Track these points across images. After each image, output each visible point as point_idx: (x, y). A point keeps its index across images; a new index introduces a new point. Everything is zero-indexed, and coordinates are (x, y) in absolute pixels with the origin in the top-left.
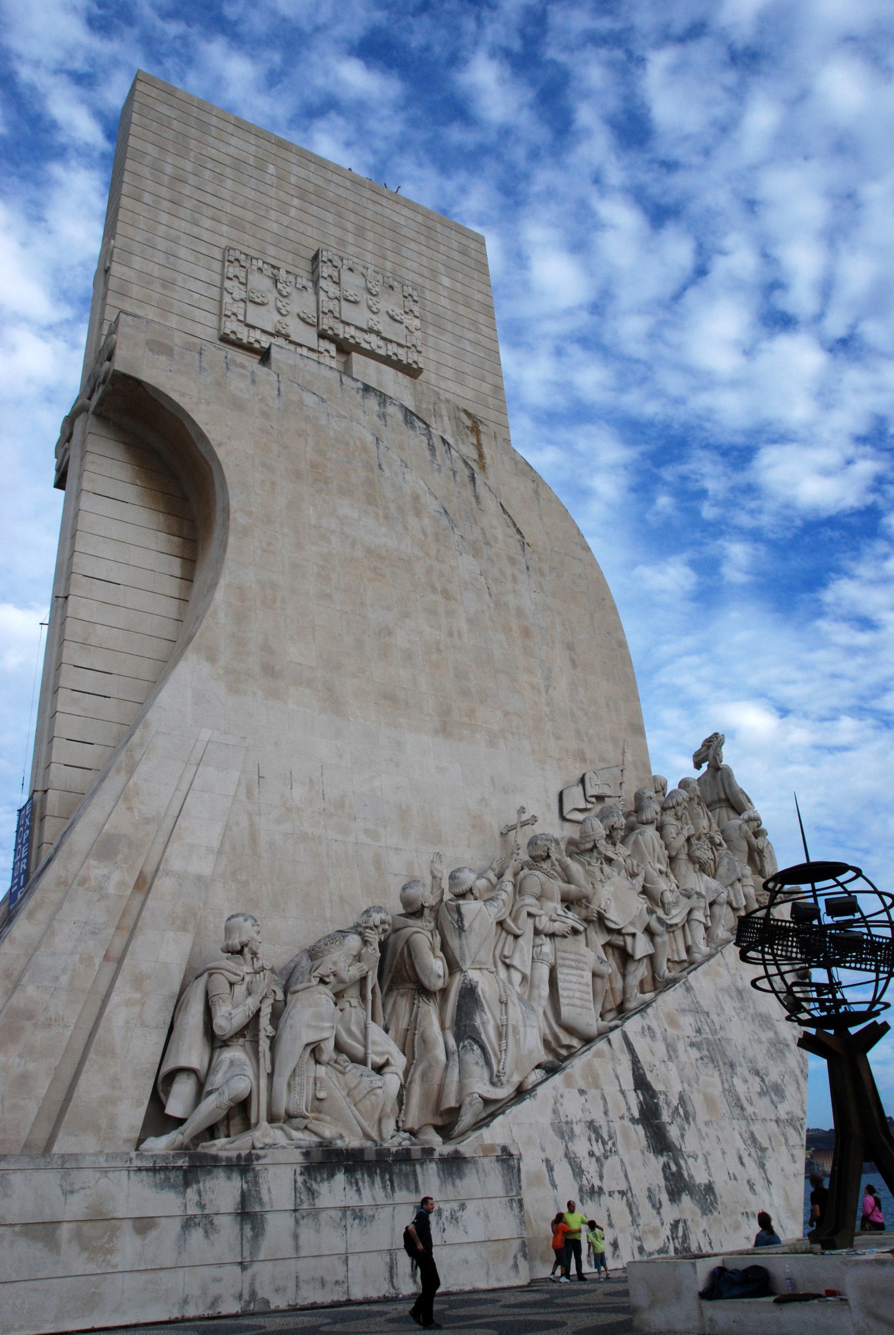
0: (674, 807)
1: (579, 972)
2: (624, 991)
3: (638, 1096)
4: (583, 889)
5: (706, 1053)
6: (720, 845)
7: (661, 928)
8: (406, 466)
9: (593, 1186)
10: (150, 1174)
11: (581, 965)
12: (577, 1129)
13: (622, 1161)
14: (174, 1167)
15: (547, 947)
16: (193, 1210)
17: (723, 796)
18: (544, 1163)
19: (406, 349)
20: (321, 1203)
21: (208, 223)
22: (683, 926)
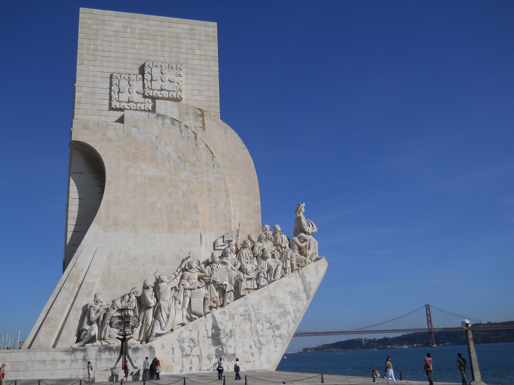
1: (198, 298)
3: (212, 331)
4: (206, 274)
6: (285, 247)
8: (167, 144)
9: (187, 354)
10: (64, 352)
11: (199, 297)
12: (186, 340)
13: (200, 348)
14: (69, 351)
15: (189, 293)
16: (73, 359)
17: (299, 226)
18: (172, 349)
19: (176, 92)
20: (102, 358)
21: (106, 64)
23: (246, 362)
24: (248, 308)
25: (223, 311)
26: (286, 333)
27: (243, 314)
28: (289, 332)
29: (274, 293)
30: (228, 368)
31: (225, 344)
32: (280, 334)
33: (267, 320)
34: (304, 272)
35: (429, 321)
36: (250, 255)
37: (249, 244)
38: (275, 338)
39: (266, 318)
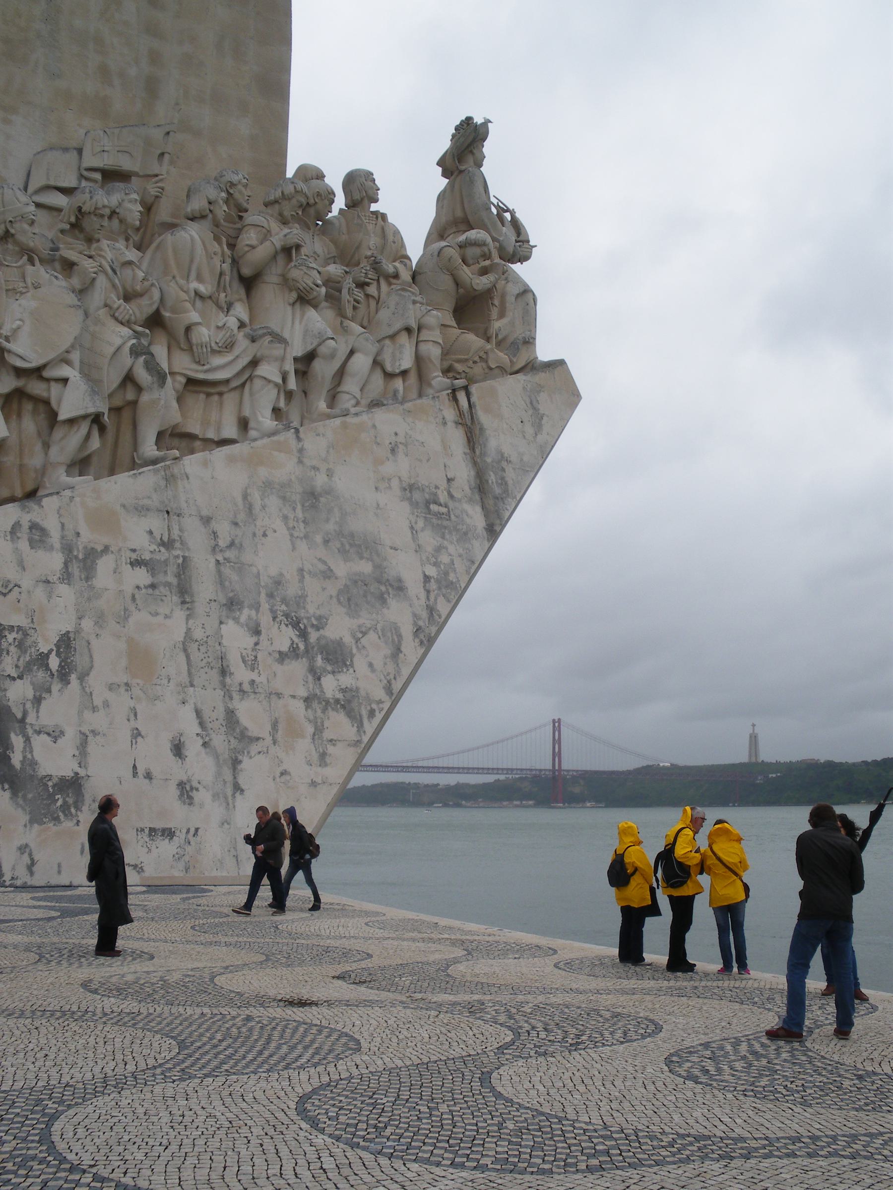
0: (276, 202)
2: (43, 471)
5: (171, 579)
6: (396, 276)
7: (149, 378)
22: (243, 385)
23: (142, 830)
24: (181, 530)
25: (26, 525)
26: (380, 694)
27: (147, 556)
28: (397, 686)
29: (330, 474)
30: (26, 859)
31: (19, 715)
32: (348, 695)
33: (284, 607)
34: (478, 407)
35: (557, 755)
36: (217, 261)
37: (221, 208)
38: (319, 711)
39: (278, 599)
